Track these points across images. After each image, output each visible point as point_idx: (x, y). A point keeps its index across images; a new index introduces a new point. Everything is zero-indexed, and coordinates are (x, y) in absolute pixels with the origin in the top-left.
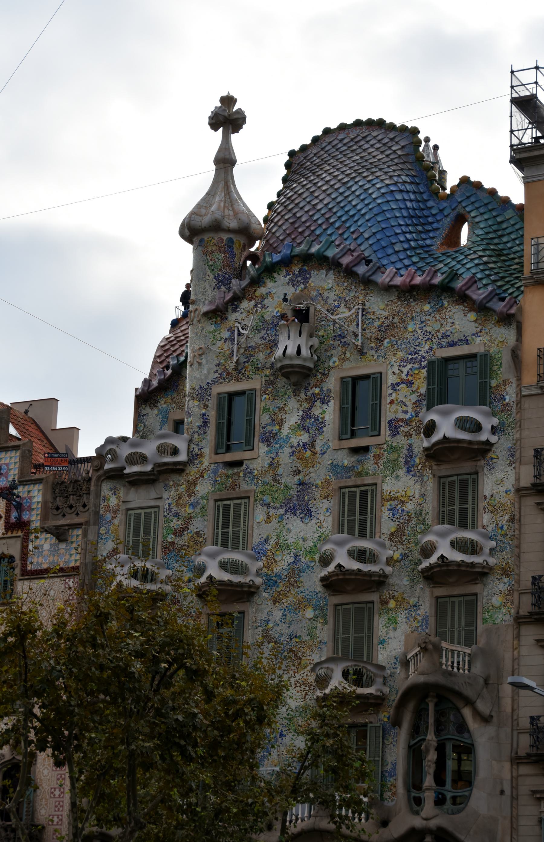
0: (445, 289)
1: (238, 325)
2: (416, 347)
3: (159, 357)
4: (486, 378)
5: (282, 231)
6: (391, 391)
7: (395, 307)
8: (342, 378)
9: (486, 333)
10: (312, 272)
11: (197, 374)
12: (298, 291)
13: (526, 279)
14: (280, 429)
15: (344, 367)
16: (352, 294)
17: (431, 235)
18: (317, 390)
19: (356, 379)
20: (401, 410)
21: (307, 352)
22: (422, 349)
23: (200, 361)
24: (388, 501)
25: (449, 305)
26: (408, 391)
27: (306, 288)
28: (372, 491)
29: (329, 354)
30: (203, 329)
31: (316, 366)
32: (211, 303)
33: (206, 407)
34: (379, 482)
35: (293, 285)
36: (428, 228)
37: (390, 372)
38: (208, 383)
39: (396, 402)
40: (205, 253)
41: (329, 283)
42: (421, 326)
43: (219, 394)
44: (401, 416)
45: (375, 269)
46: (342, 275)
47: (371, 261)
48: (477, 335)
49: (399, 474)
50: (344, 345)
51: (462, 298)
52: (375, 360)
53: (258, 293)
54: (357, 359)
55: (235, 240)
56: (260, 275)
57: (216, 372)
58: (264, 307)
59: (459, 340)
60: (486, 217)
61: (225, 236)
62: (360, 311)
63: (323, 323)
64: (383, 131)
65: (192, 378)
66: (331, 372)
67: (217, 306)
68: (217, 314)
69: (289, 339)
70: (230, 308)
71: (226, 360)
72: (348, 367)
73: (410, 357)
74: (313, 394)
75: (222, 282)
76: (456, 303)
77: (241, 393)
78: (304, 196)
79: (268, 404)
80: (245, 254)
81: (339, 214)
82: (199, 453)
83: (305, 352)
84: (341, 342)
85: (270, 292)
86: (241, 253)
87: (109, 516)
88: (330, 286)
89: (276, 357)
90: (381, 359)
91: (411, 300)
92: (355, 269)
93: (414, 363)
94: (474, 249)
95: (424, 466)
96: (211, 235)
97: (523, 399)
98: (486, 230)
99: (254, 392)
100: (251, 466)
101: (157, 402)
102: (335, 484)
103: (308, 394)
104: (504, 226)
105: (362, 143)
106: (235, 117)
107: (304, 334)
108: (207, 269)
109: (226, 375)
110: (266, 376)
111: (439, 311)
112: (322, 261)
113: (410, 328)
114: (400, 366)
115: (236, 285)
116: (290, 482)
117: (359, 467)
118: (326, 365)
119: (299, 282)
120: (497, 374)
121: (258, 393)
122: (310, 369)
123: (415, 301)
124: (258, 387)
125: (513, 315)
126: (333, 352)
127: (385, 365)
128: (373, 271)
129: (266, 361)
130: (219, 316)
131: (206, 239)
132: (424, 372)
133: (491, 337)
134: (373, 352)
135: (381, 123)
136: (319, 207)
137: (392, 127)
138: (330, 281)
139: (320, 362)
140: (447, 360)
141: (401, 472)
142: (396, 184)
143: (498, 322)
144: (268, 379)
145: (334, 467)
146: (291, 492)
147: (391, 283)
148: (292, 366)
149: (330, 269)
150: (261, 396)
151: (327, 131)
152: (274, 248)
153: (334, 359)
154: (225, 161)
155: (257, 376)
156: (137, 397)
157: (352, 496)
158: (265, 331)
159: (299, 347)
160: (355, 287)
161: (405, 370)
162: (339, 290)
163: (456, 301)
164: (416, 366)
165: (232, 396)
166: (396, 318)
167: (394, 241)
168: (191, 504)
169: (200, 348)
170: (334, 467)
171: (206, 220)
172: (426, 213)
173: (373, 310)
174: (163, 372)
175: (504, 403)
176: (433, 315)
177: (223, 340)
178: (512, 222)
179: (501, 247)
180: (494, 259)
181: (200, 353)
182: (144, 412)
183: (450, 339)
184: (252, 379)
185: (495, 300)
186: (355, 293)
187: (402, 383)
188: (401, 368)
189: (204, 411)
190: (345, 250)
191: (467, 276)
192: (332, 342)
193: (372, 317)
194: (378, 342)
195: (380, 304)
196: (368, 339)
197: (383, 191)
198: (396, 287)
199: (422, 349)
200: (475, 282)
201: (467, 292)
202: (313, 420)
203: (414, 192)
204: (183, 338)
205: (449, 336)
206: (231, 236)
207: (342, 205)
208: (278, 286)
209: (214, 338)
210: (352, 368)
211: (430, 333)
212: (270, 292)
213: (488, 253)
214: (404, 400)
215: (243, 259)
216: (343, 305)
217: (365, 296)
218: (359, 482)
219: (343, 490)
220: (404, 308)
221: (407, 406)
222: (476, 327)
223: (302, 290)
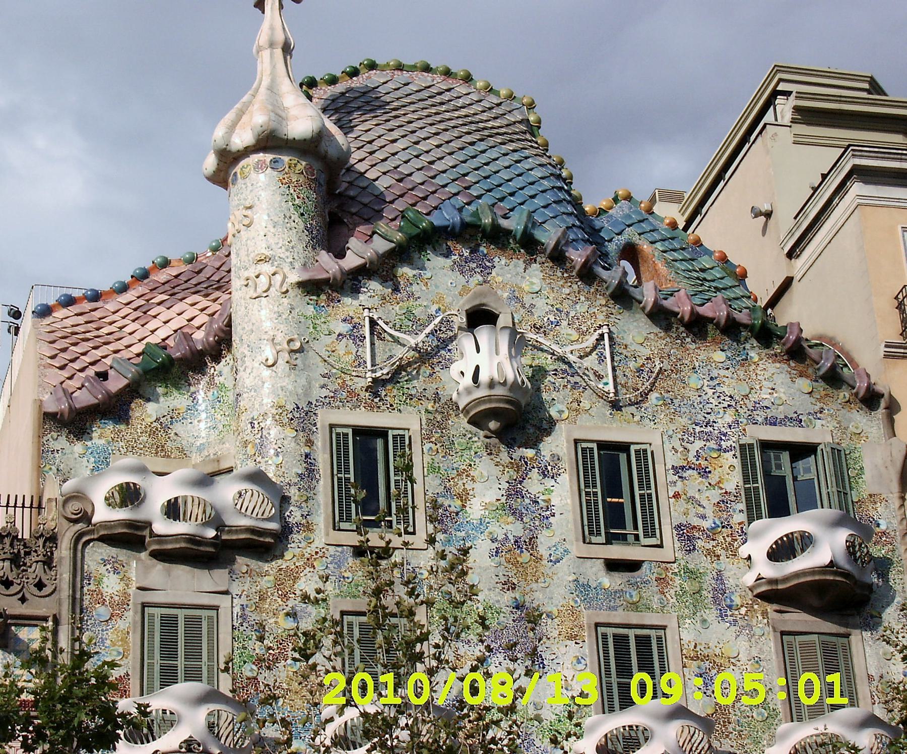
8: (576, 442)
9: (831, 416)
14: (464, 506)
16: (581, 308)
18: (530, 453)
22: (719, 420)
24: (692, 659)
27: (485, 282)
28: (659, 638)
34: (672, 624)
41: (532, 283)
43: (332, 426)
44: (696, 522)
46: (560, 274)
49: (705, 617)
50: (573, 388)
52: (638, 423)
54: (605, 415)
59: (786, 417)
73: (698, 429)
79: (436, 460)
82: (304, 521)
84: (569, 381)
87: (102, 612)
88: (538, 289)
91: (688, 340)
93: (707, 440)
95: (750, 609)
100: (414, 563)
102: (587, 617)
108: (292, 209)
110: (427, 411)
113: (694, 381)
116: (498, 601)
117: (634, 593)
134: (633, 409)
140: (766, 446)
141: (711, 615)
145: (582, 588)
146: (501, 619)
155: (411, 409)
157: (621, 642)
160: (588, 299)
164: (712, 444)
168: (288, 614)
170: (582, 588)
177: (335, 336)
189: (307, 450)
193: (624, 352)
199: (719, 420)
202: (527, 501)
211: (731, 396)
216: (564, 323)
217: (608, 317)
218: (634, 618)
219: (601, 630)
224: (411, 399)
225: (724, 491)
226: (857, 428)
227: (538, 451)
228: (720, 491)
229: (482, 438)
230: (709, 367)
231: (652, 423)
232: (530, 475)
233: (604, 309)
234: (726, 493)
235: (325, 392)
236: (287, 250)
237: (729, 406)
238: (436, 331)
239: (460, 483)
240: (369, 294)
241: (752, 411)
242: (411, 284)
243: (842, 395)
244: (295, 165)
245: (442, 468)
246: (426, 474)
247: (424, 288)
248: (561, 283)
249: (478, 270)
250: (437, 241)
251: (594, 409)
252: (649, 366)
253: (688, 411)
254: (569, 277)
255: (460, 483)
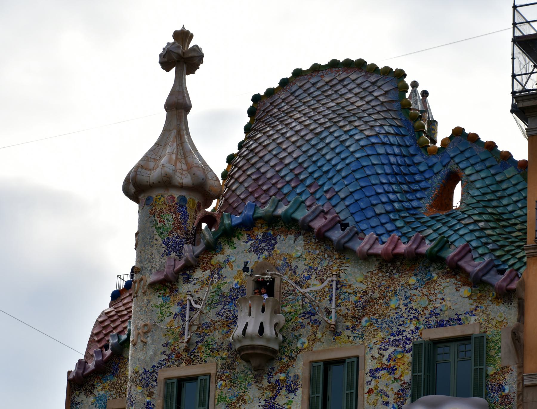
0: (435, 259)
1: (190, 298)
2: (399, 327)
3: (97, 334)
4: (481, 364)
5: (244, 189)
6: (370, 379)
7: (375, 279)
8: (312, 362)
9: (482, 311)
10: (278, 237)
11: (141, 355)
12: (261, 260)
13: (529, 248)
15: (314, 349)
17: (418, 195)
18: (282, 376)
19: (328, 364)
20: (380, 400)
21: (271, 331)
22: (407, 330)
23: (145, 340)
25: (438, 278)
26: (390, 378)
27: (270, 255)
29: (296, 333)
30: (149, 302)
31: (281, 347)
32: (158, 271)
33: (151, 394)
35: (256, 252)
36: (415, 187)
37: (369, 356)
38: (154, 366)
39: (375, 391)
40: (153, 213)
41: (297, 251)
42: (405, 302)
43: (166, 379)
45: (352, 234)
46: (313, 241)
47: (347, 225)
48: (471, 313)
51: (454, 270)
52: (351, 342)
53: (214, 262)
55: (188, 198)
56: (217, 239)
57: (164, 353)
58: (220, 277)
59: (450, 319)
60: (483, 175)
61: (176, 194)
62: (334, 284)
63: (291, 297)
64: (363, 73)
65: (135, 360)
66: (299, 355)
67: (166, 276)
68: (166, 285)
69: (250, 315)
70: (181, 278)
71: (175, 339)
72: (319, 349)
73: (392, 338)
74: (277, 381)
75: (172, 247)
76: (448, 275)
77: (193, 379)
78: (270, 148)
79: (224, 392)
80: (200, 215)
81: (310, 170)
83: (269, 331)
84: (311, 320)
85: (228, 260)
86: (195, 214)
89: (235, 336)
90: (358, 340)
91: (394, 271)
92: (328, 234)
93: (397, 346)
94: (469, 213)
96: (160, 192)
97: (526, 390)
98: (482, 191)
99: (208, 377)
101: (93, 387)
103: (272, 380)
104: (504, 186)
105: (339, 87)
106: (190, 55)
107: (268, 311)
108: (155, 232)
109: (175, 357)
110: (222, 358)
111: (427, 284)
112: (291, 225)
114: (380, 349)
115: (189, 251)
118: (293, 347)
119: (263, 249)
120: (495, 360)
121: (213, 379)
122: (274, 351)
123: (398, 272)
124: (213, 371)
125: (514, 291)
126: (302, 331)
127: (363, 347)
128: (350, 237)
129: (222, 341)
130: (168, 287)
131: (154, 196)
132: (409, 357)
133: (488, 316)
134: (349, 332)
135: (360, 64)
136: (287, 161)
137: (374, 69)
138: (299, 248)
139: (286, 344)
140: (436, 343)
142: (377, 135)
143: (497, 298)
144: (224, 362)
147: (371, 251)
148: (253, 347)
149: (300, 233)
150: (216, 382)
151: (297, 73)
152: (234, 208)
153: (303, 339)
154: (178, 106)
155: (212, 359)
156: (70, 382)
158: (222, 306)
159: (262, 325)
161: (386, 354)
162: (310, 259)
163: (447, 273)
164: (400, 349)
165: (182, 381)
166: (376, 292)
167: (374, 202)
169: (146, 325)
171: (154, 175)
172: (412, 169)
173: (349, 283)
174: (100, 352)
175: (503, 394)
176: (419, 289)
177: (172, 316)
178: (514, 182)
179: (500, 210)
180: (492, 225)
181: (145, 330)
182: (78, 399)
183: (440, 318)
184: (206, 361)
185: (492, 272)
186: (328, 262)
187: (383, 369)
188: (381, 352)
189: (148, 399)
190: (317, 212)
191: (460, 244)
192: (300, 320)
193: (348, 290)
194: (354, 320)
195: (358, 275)
196: (343, 316)
197: (362, 143)
198: (376, 256)
199: (407, 330)
200: (470, 251)
201: (460, 263)
203: (399, 146)
204: (125, 312)
205: (438, 314)
206: (184, 193)
207: (314, 159)
208: (238, 253)
209: (161, 313)
210: (323, 351)
211: (416, 310)
212: (228, 260)
213: (485, 217)
214: (385, 389)
215: (197, 221)
217: (340, 266)
220: (386, 280)
221: (388, 397)
222: (470, 304)
223: (266, 258)
224: (213, 352)
225: (403, 382)
226: (501, 317)
227: (288, 375)
228: (400, 383)
229: (253, 372)
230: (406, 290)
231: (361, 340)
232: (281, 392)
233: (338, 261)
234: (404, 383)
235: (164, 357)
236: (149, 262)
237: (414, 317)
238: (234, 299)
239: (238, 405)
240: (193, 282)
241: (428, 318)
242: (222, 269)
243: (491, 295)
244: (160, 199)
245: (228, 397)
246: (216, 403)
247: (230, 269)
248: (315, 247)
249: (266, 248)
250: (240, 233)
251: (324, 337)
252: (365, 297)
253: (387, 326)
254: (319, 242)
255: (238, 405)
